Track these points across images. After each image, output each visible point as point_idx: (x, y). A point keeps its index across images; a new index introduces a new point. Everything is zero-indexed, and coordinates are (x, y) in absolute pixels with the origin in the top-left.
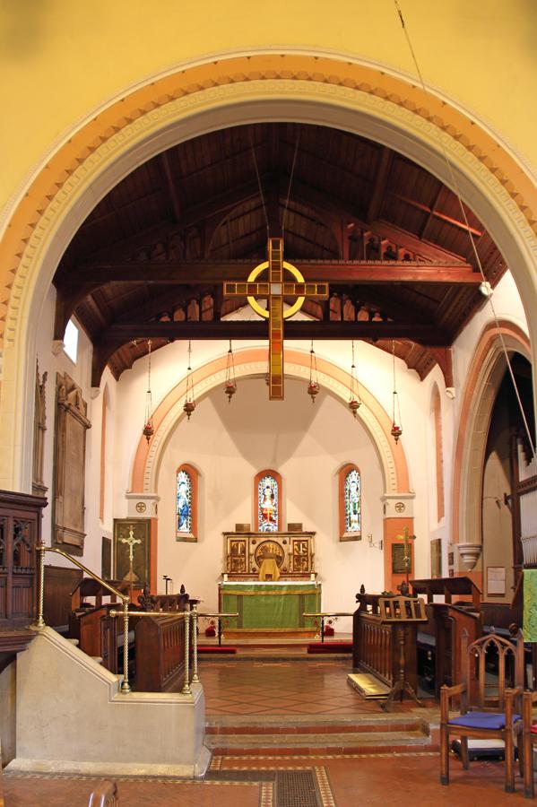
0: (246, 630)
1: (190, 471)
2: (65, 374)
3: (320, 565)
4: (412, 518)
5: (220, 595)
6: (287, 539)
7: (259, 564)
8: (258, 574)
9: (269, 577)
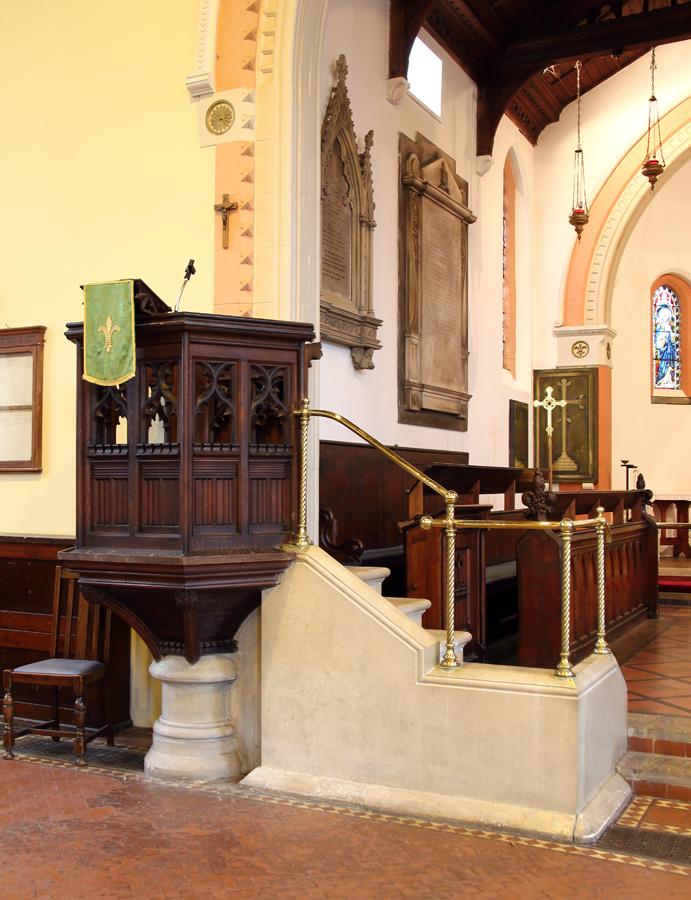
2: (418, 135)
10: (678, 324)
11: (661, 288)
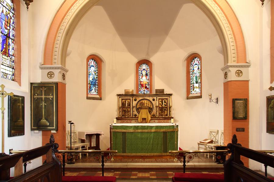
0: (129, 154)
1: (96, 59)
3: (173, 113)
4: (248, 81)
5: (111, 132)
6: (155, 98)
7: (139, 112)
8: (138, 118)
9: (144, 121)
10: (97, 73)
11: (91, 60)
